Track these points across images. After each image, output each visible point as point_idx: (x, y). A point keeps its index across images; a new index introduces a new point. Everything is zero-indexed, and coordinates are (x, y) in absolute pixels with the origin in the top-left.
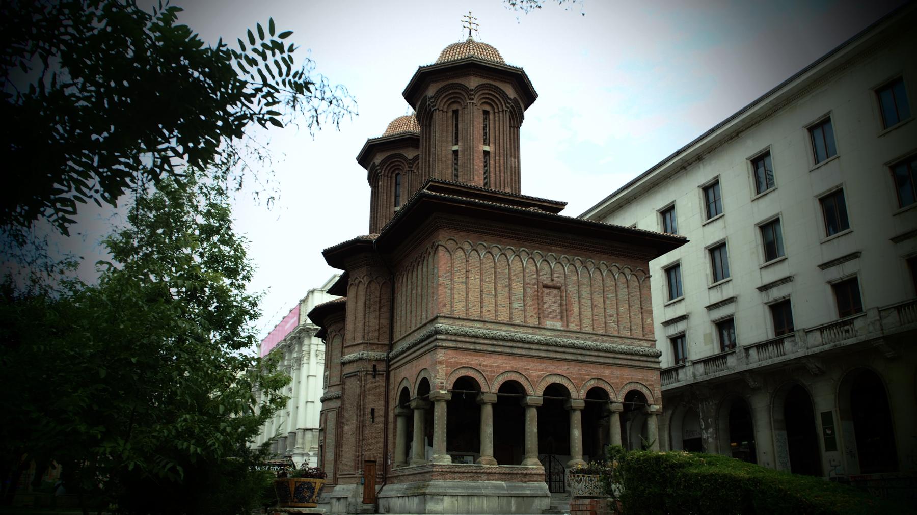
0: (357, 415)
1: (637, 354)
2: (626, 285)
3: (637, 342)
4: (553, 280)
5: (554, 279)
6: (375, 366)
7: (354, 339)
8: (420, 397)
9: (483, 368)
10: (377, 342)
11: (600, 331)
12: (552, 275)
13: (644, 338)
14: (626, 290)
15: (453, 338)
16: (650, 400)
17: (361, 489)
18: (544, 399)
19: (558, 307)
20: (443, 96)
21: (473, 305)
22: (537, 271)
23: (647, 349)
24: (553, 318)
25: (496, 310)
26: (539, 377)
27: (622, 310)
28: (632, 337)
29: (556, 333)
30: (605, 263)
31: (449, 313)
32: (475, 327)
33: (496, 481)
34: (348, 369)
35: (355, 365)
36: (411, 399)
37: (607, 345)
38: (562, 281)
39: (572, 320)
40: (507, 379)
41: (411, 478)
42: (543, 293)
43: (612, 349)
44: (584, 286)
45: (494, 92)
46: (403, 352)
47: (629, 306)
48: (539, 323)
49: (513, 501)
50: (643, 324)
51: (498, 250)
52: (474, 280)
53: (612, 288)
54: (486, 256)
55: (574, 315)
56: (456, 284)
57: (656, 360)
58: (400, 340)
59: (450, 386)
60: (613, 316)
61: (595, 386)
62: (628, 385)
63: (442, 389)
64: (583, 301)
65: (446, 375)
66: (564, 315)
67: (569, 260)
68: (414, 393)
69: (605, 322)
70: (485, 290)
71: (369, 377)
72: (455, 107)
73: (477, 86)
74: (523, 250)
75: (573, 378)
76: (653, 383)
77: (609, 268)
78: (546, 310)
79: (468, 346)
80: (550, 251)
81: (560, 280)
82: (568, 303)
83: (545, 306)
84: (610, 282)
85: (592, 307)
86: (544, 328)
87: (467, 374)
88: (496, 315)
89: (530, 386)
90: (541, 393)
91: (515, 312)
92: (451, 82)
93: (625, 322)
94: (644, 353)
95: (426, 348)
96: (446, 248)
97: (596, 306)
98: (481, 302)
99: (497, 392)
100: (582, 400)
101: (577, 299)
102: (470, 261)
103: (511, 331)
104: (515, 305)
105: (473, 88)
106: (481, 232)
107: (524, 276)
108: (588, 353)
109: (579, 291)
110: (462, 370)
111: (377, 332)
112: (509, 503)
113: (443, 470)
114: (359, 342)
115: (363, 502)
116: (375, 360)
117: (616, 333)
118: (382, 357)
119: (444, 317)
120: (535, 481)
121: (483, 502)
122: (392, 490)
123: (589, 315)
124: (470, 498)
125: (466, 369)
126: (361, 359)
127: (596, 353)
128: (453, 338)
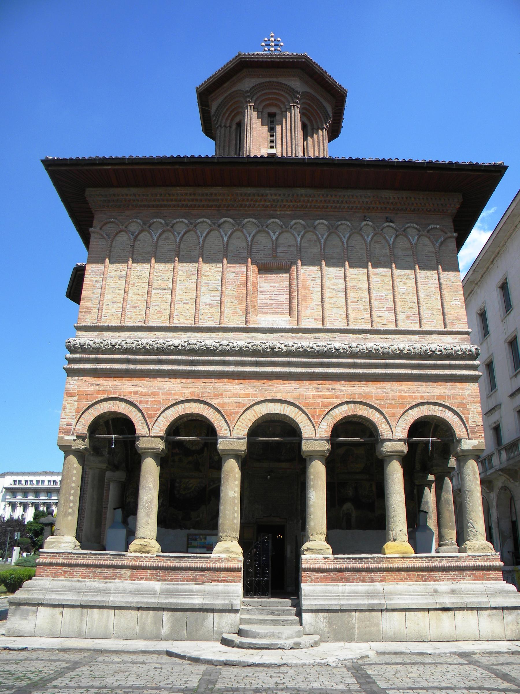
2: (410, 253)
9: (140, 398)
18: (249, 443)
19: (285, 296)
20: (224, 111)
21: (135, 307)
24: (277, 313)
33: (147, 579)
39: (308, 312)
40: (182, 413)
43: (381, 350)
45: (278, 89)
47: (416, 283)
49: (166, 615)
54: (164, 236)
56: (109, 280)
59: (83, 428)
60: (386, 300)
61: (350, 413)
62: (416, 409)
63: (67, 433)
65: (77, 412)
72: (237, 120)
73: (254, 87)
74: (225, 222)
83: (261, 296)
89: (223, 422)
90: (246, 432)
92: (229, 93)
96: (102, 235)
100: (321, 439)
102: (136, 246)
105: (248, 89)
106: (157, 206)
112: (159, 622)
113: (54, 561)
117: (392, 327)
120: (222, 581)
121: (108, 617)
124: (85, 610)
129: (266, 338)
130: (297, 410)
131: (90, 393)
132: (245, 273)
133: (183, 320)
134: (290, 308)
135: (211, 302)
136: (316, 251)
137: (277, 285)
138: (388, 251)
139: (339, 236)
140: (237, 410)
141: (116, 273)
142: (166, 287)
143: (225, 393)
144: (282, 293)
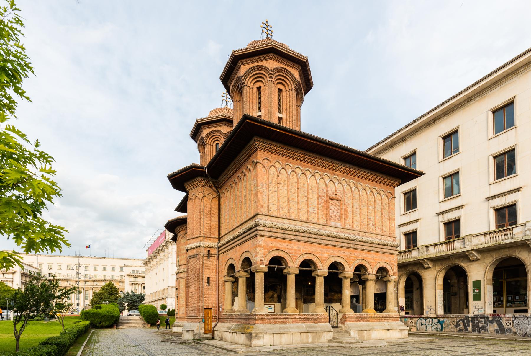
0: (198, 281)
1: (385, 245)
2: (381, 202)
3: (385, 238)
4: (336, 194)
5: (337, 194)
6: (209, 251)
7: (193, 234)
8: (242, 270)
10: (210, 236)
11: (364, 230)
12: (336, 191)
13: (390, 235)
14: (380, 205)
15: (269, 229)
16: (391, 273)
17: (203, 325)
18: (329, 272)
22: (326, 187)
23: (391, 242)
25: (298, 212)
26: (326, 258)
27: (377, 218)
28: (383, 234)
29: (337, 229)
30: (369, 186)
31: (266, 212)
32: (284, 223)
34: (191, 253)
35: (195, 250)
36: (236, 271)
37: (368, 239)
38: (342, 195)
39: (347, 222)
41: (237, 320)
42: (329, 203)
43: (371, 241)
44: (355, 200)
46: (229, 242)
48: (327, 223)
50: (389, 227)
51: (300, 171)
52: (284, 191)
53: (373, 203)
54: (292, 174)
55: (349, 219)
56: (270, 192)
57: (396, 249)
58: (226, 235)
60: (372, 221)
61: (360, 264)
64: (355, 210)
66: (343, 216)
67: (346, 182)
68: (238, 266)
69: (368, 224)
70: (291, 198)
71: (206, 258)
74: (317, 172)
75: (347, 259)
76: (393, 263)
77: (371, 190)
78: (331, 214)
79: (279, 235)
80: (334, 174)
81: (340, 195)
82: (346, 210)
83: (330, 212)
84: (371, 199)
85: (360, 215)
86: (330, 226)
87: (279, 255)
88: (299, 216)
90: (328, 268)
91: (311, 214)
93: (379, 225)
94: (390, 244)
95: (248, 237)
97: (362, 214)
98: (289, 206)
99: (299, 266)
101: (351, 208)
103: (308, 227)
104: (311, 210)
107: (317, 190)
108: (357, 243)
109: (352, 203)
110: (275, 251)
111: (210, 229)
114: (197, 236)
115: (204, 333)
116: (209, 248)
117: (373, 232)
118: (213, 246)
119: (262, 215)
122: (224, 327)
123: (358, 219)
125: (277, 251)
126: (199, 247)
127: (362, 243)
128: (269, 229)
129: (333, 230)
130: (344, 261)
131: (268, 246)
132: (325, 200)
133: (303, 218)
134: (341, 219)
135: (313, 211)
136: (350, 194)
137: (336, 207)
138: (374, 200)
139: (358, 189)
140: (324, 259)
141: (272, 189)
142: (295, 201)
143: (321, 252)
144: (337, 211)
